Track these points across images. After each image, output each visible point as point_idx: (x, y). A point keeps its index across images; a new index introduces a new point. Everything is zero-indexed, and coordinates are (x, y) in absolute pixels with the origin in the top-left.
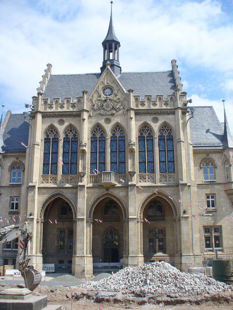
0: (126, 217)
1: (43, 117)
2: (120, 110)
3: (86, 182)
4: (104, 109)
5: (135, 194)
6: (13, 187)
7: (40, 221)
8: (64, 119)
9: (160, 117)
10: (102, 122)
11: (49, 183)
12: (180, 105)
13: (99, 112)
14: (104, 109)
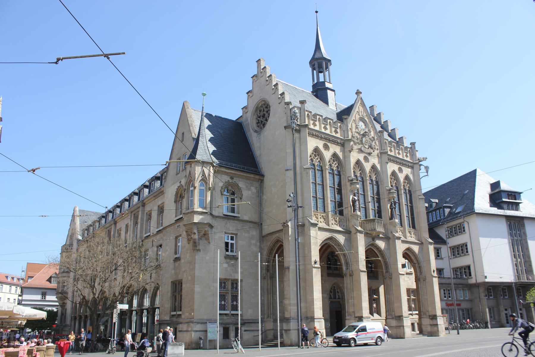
0: (387, 272)
6: (228, 219)
8: (329, 144)
9: (403, 168)
13: (359, 147)
14: (362, 143)
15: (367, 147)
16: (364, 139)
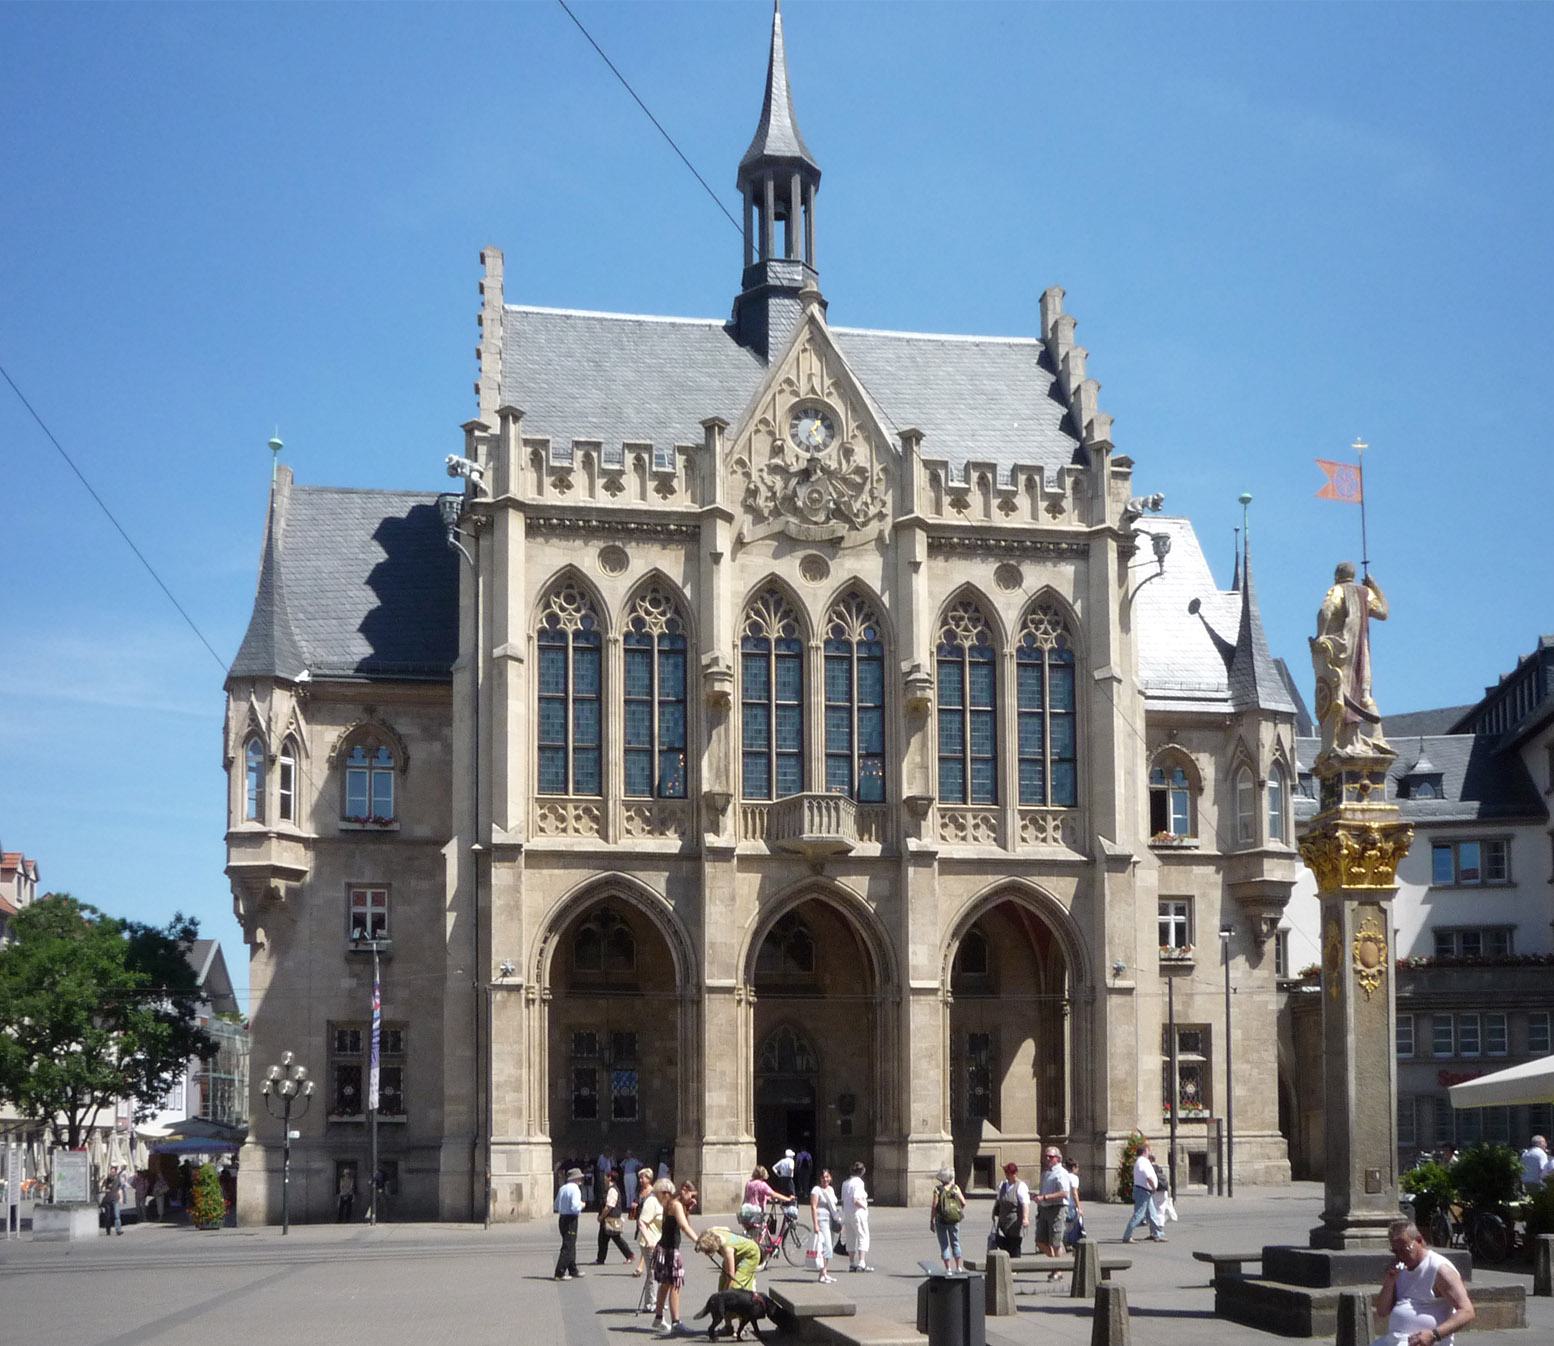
0: (887, 978)
1: (531, 530)
2: (864, 524)
3: (732, 834)
4: (796, 511)
5: (933, 891)
7: (537, 996)
10: (790, 569)
11: (570, 831)
12: (1112, 521)
15: (821, 517)
16: (803, 492)
